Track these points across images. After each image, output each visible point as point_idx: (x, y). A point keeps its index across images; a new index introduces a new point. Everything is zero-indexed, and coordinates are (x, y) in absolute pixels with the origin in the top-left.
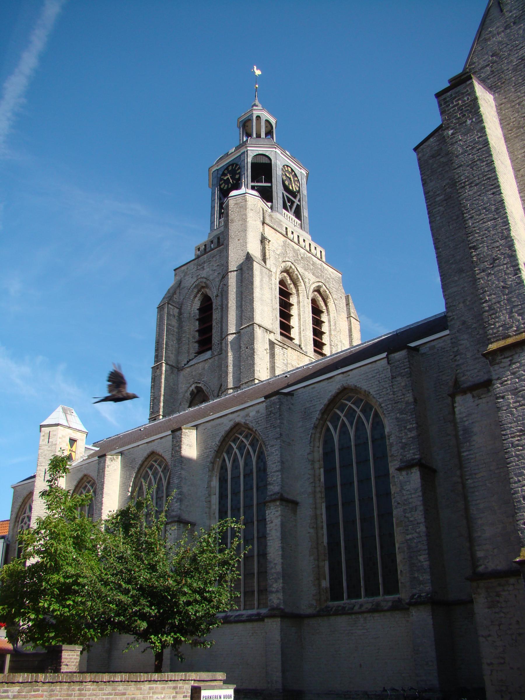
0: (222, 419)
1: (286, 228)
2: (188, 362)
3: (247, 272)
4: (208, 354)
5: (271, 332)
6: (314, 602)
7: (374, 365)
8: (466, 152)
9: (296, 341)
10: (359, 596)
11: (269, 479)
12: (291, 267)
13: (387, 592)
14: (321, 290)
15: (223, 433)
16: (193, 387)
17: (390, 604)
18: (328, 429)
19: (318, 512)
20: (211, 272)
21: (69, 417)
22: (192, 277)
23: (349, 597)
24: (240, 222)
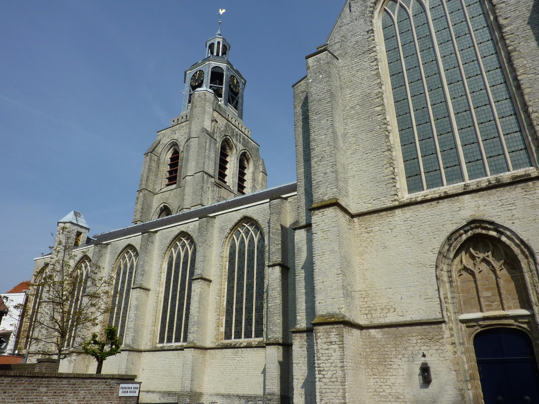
0: (173, 228)
1: (229, 115)
2: (161, 190)
4: (174, 186)
5: (212, 177)
6: (214, 340)
7: (262, 205)
8: (317, 93)
9: (227, 184)
10: (240, 338)
11: (196, 266)
12: (229, 139)
13: (256, 336)
14: (246, 155)
15: (173, 236)
16: (162, 205)
17: (257, 343)
18: (234, 239)
19: (222, 287)
20: (180, 136)
21: (78, 218)
23: (235, 338)
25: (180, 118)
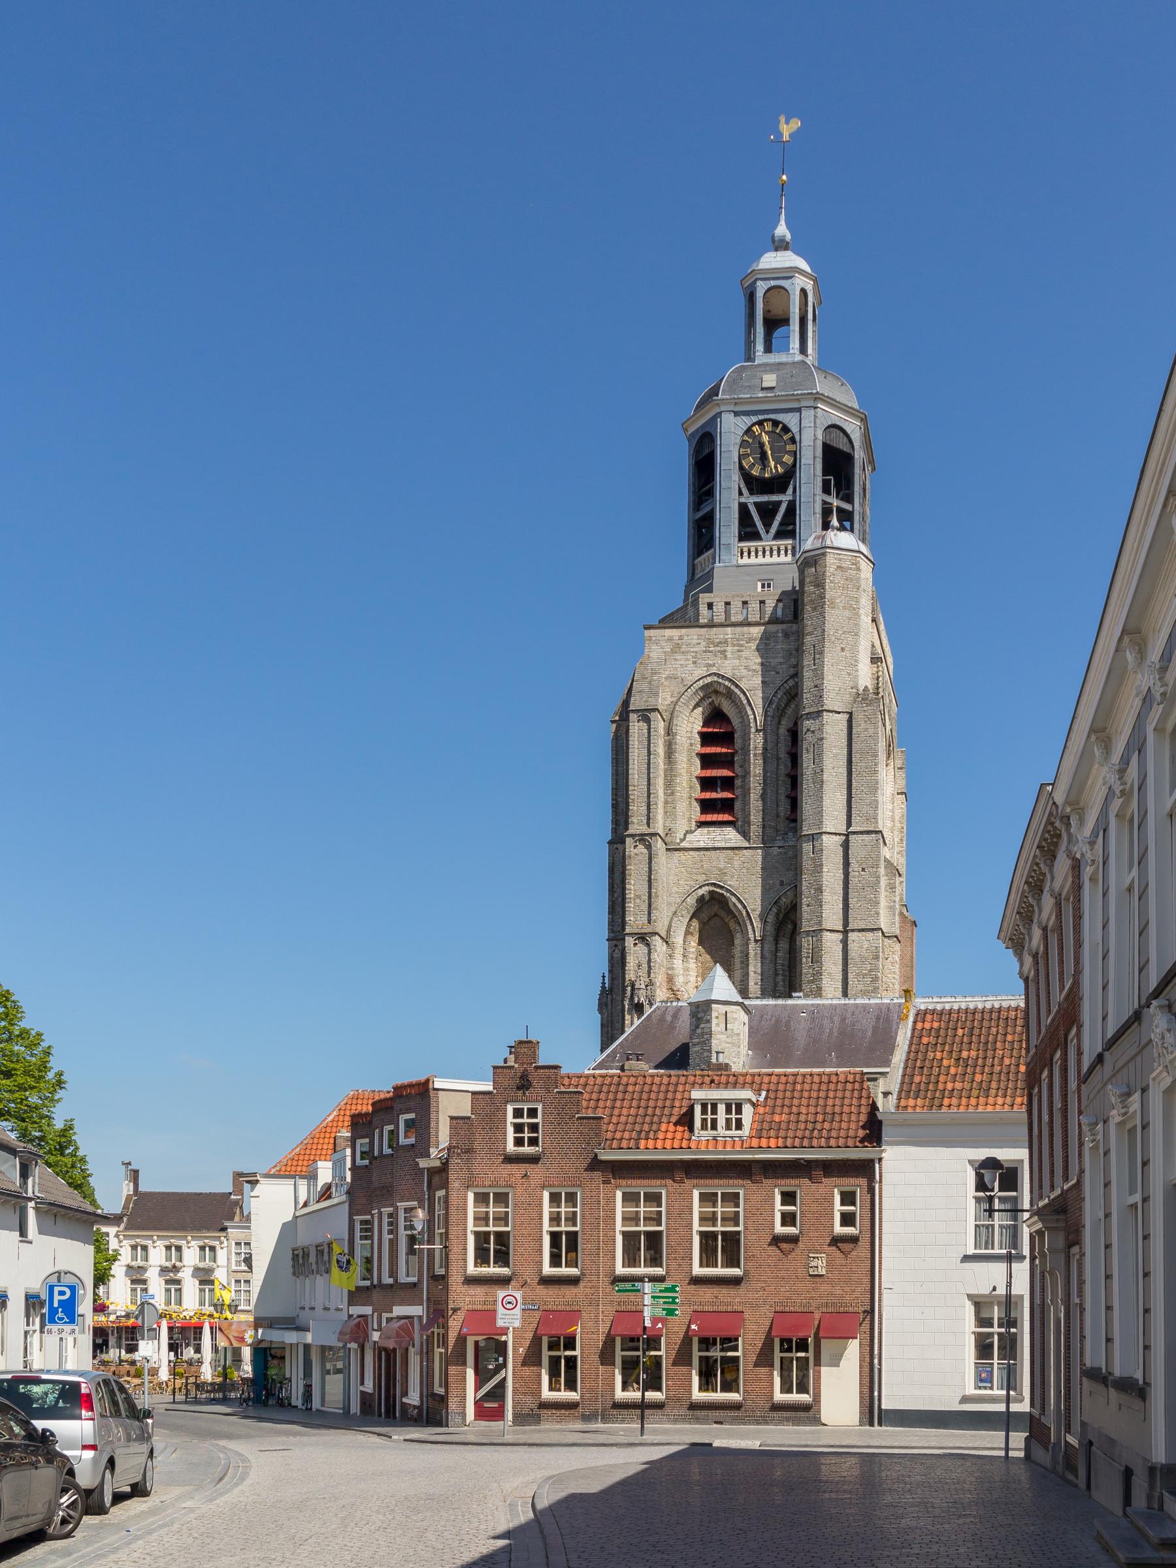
3: (863, 725)
16: (707, 888)
20: (744, 672)
22: (694, 663)
24: (847, 613)
25: (736, 605)
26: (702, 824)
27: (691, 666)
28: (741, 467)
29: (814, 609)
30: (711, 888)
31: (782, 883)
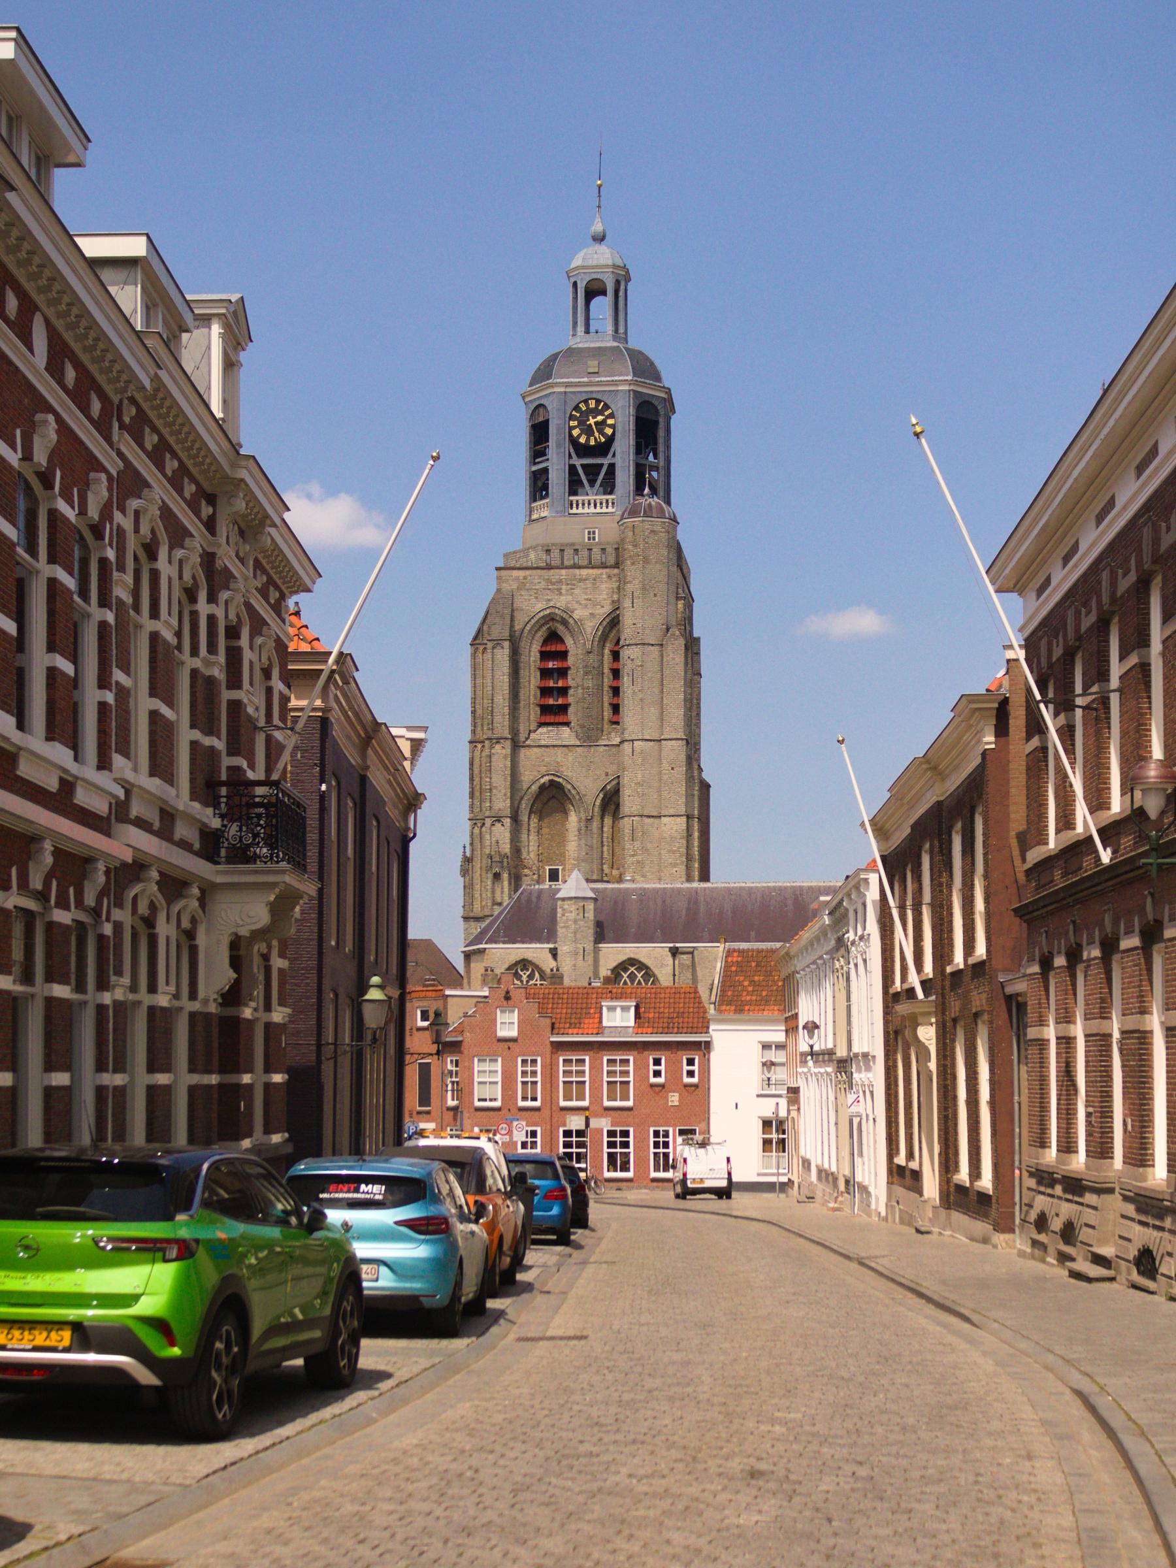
16: (546, 779)
24: (658, 566)
26: (541, 724)
27: (533, 601)
28: (571, 435)
29: (633, 564)
30: (551, 777)
31: (607, 774)
